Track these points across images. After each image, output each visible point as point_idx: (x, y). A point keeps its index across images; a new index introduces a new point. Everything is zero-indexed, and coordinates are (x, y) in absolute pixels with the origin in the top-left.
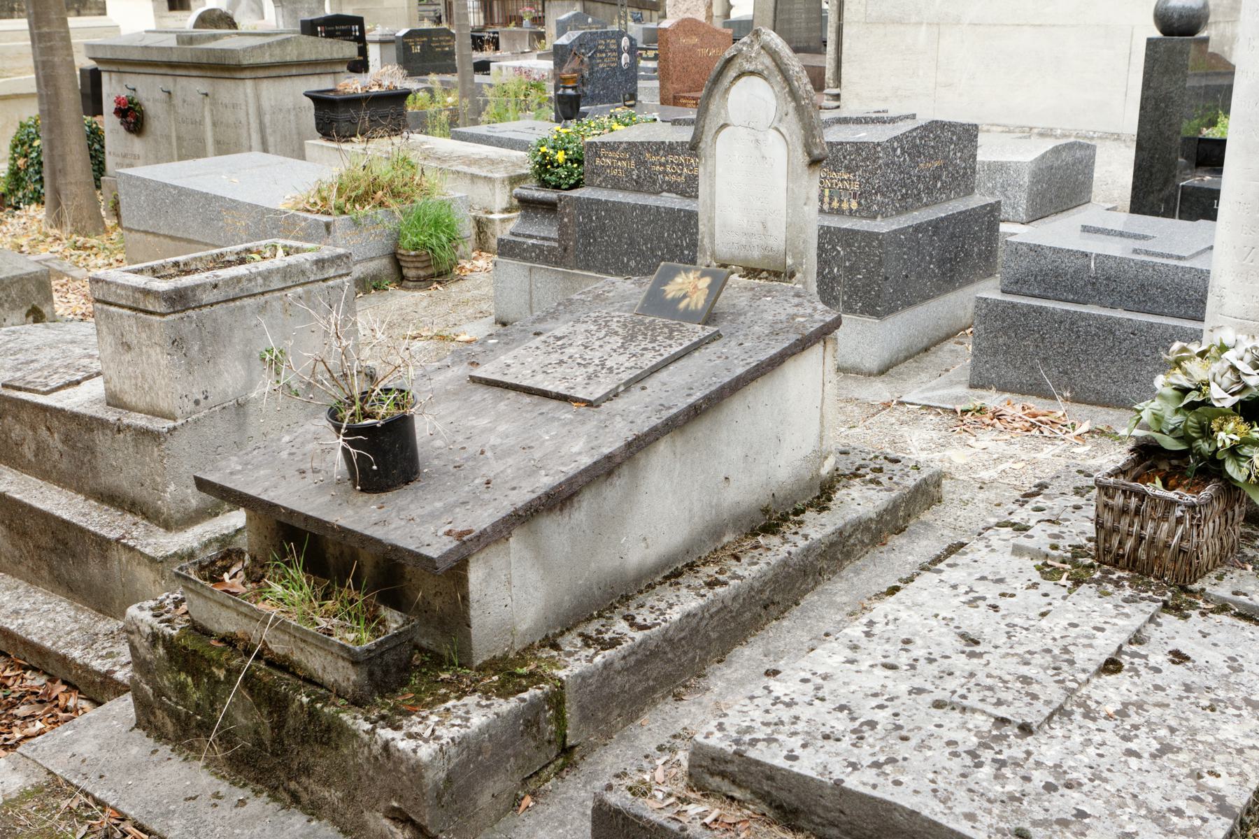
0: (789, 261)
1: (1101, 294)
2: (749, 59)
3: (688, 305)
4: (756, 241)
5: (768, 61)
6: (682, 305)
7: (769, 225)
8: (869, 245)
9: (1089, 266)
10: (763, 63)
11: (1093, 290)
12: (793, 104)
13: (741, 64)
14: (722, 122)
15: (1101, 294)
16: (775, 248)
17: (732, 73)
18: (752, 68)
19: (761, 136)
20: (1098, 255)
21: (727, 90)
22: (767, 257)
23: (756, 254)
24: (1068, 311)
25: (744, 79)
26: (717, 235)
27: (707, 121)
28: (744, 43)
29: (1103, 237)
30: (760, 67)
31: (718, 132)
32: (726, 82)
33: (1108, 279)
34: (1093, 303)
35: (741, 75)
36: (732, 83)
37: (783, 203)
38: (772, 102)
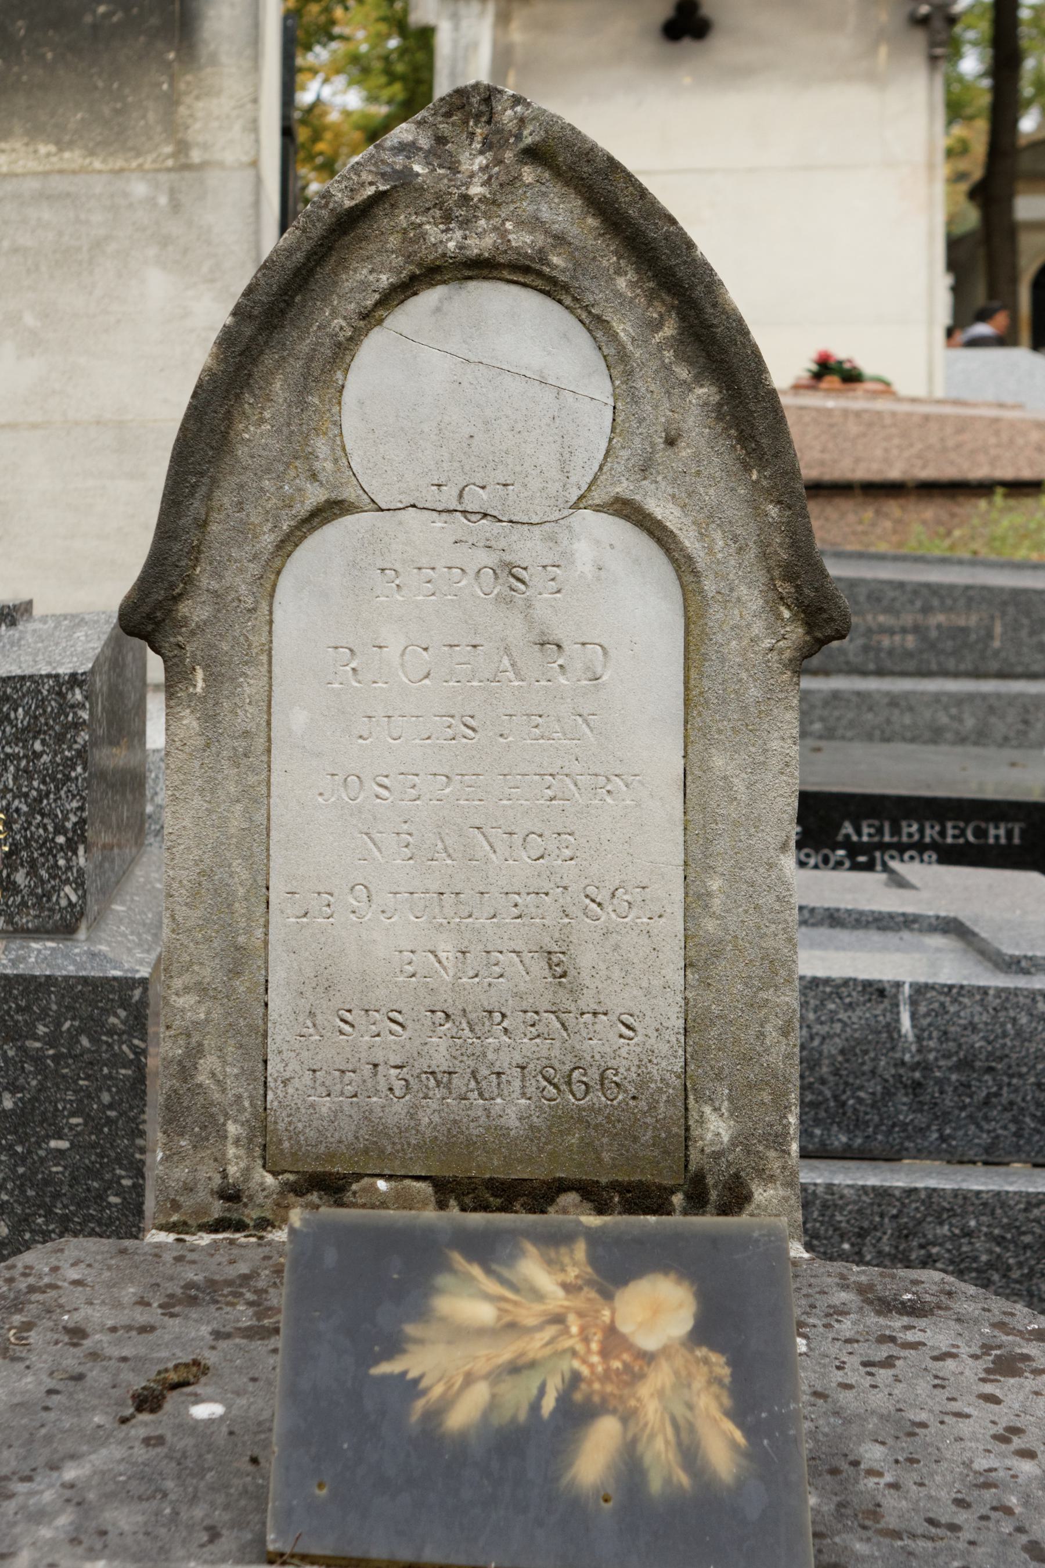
0: (716, 1128)
1: (945, 1117)
2: (455, 210)
3: (630, 1465)
4: (506, 1049)
5: (561, 211)
6: (593, 1459)
7: (586, 959)
8: (93, 1026)
9: (892, 1028)
10: (535, 223)
11: (918, 1107)
12: (705, 392)
13: (414, 236)
14: (315, 496)
15: (945, 1117)
16: (626, 1068)
17: (368, 274)
18: (481, 243)
19: (528, 548)
20: (920, 990)
21: (343, 350)
22: (579, 1118)
23: (513, 1108)
24: (882, 1194)
25: (430, 298)
26: (280, 1036)
27: (225, 498)
28: (407, 149)
29: (875, 937)
30: (522, 240)
31: (288, 543)
32: (334, 315)
33: (965, 1064)
34: (920, 1154)
35: (427, 274)
36: (369, 319)
37: (664, 848)
38: (592, 391)
